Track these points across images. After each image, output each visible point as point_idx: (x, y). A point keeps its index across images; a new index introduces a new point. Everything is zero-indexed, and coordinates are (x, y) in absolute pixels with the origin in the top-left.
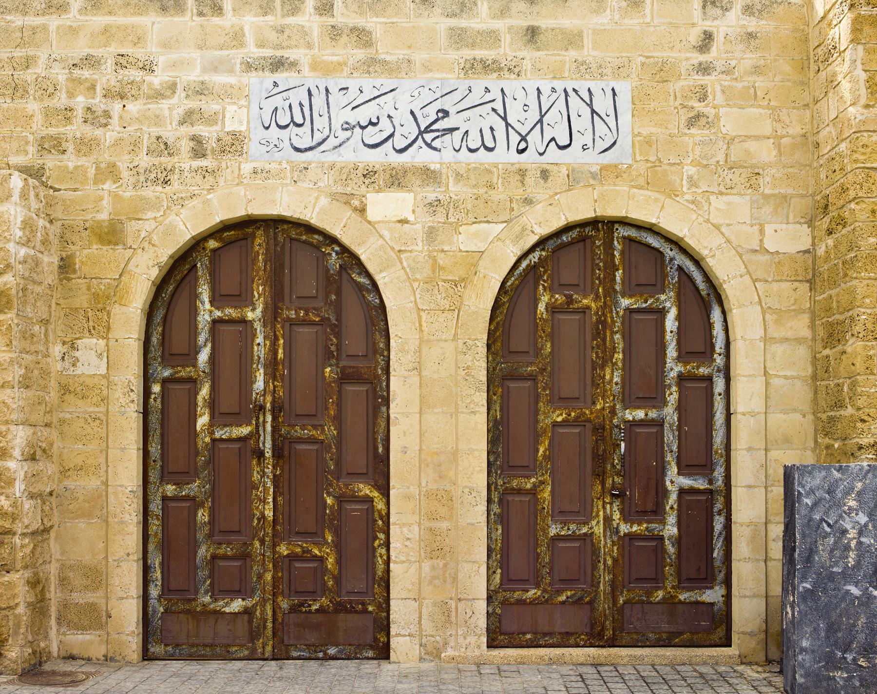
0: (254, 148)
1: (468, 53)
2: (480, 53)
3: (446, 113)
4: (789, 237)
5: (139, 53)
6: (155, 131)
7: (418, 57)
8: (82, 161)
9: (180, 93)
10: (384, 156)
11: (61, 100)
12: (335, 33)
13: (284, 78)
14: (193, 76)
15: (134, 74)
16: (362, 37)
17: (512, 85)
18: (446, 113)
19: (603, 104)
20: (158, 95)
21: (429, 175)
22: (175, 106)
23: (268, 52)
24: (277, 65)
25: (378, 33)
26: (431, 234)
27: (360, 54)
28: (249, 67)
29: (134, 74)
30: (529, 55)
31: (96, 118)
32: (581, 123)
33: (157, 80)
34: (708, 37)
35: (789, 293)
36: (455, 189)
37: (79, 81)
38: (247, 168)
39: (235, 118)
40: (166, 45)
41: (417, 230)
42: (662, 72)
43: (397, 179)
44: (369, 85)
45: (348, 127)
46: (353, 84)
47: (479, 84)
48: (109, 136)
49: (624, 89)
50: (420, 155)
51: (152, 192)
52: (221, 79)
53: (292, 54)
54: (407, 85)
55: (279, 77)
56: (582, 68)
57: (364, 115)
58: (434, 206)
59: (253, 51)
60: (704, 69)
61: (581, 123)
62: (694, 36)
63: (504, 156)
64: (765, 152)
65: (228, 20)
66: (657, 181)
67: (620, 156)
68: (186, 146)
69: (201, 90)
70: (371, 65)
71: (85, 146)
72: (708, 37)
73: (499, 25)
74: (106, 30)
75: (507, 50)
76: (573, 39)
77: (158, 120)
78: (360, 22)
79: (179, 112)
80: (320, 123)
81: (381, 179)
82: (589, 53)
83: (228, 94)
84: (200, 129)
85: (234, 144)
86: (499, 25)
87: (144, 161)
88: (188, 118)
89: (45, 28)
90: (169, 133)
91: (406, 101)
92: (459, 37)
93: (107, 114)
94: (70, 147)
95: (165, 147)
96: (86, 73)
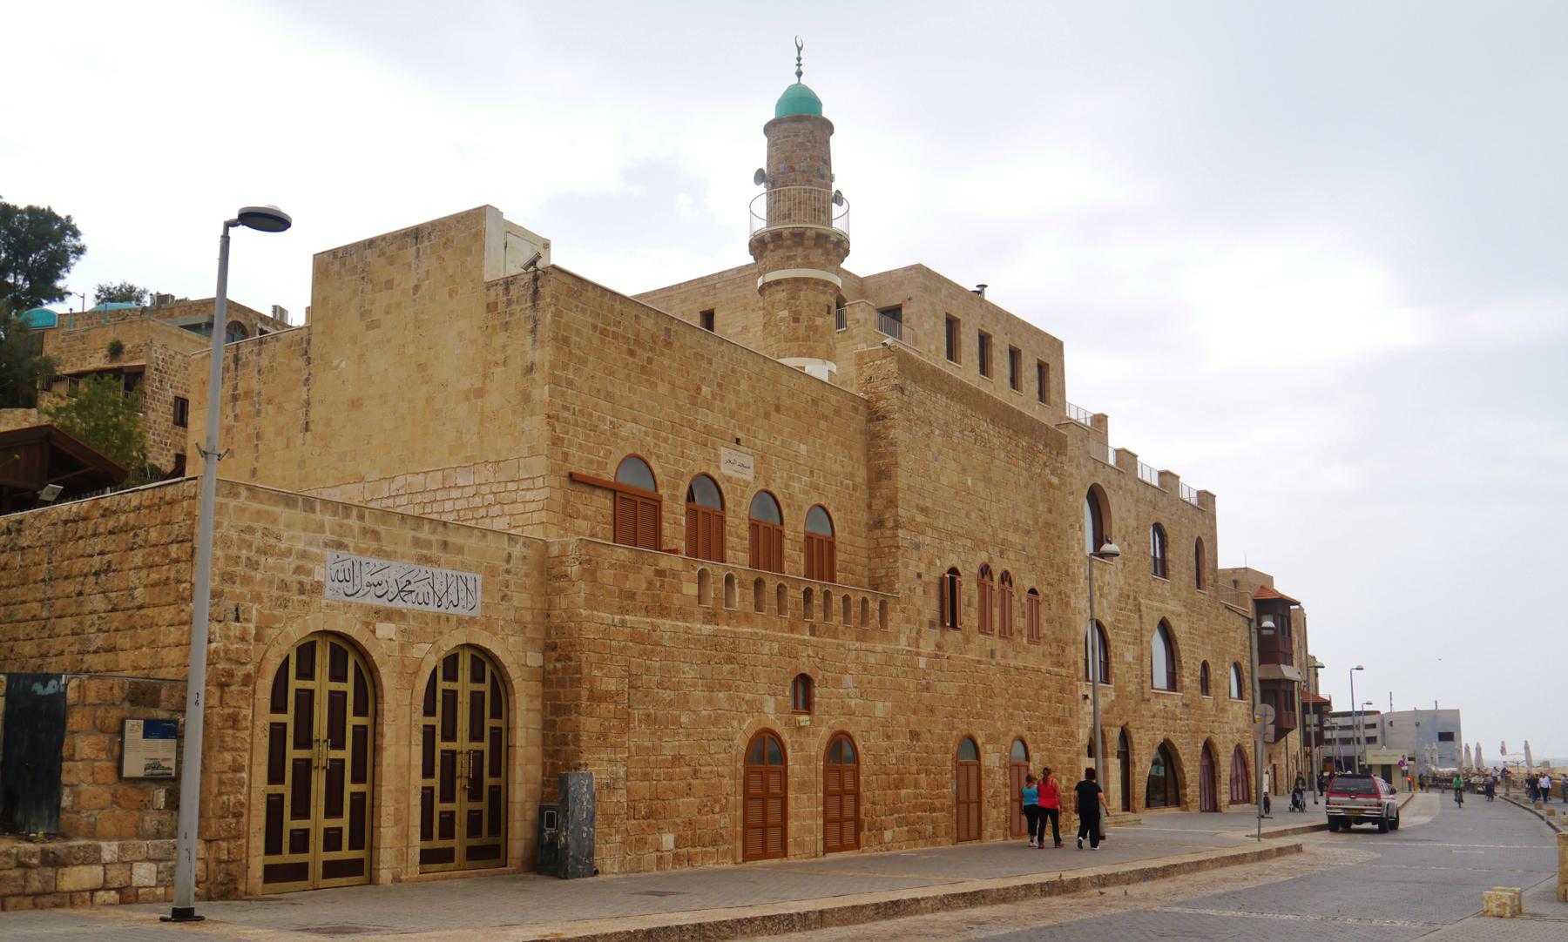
0: (327, 592)
1: (420, 551)
2: (425, 552)
3: (409, 582)
4: (535, 659)
5: (274, 528)
6: (281, 576)
7: (400, 550)
8: (244, 590)
9: (294, 555)
10: (382, 603)
11: (234, 551)
12: (365, 531)
13: (343, 554)
14: (300, 546)
15: (272, 541)
16: (376, 535)
17: (436, 570)
18: (409, 582)
19: (471, 586)
20: (283, 555)
21: (401, 615)
22: (291, 563)
23: (334, 538)
24: (340, 546)
25: (383, 534)
26: (402, 647)
27: (375, 545)
28: (326, 545)
29: (272, 541)
30: (444, 557)
31: (252, 564)
32: (462, 594)
33: (283, 546)
34: (510, 556)
35: (535, 687)
36: (413, 624)
37: (244, 541)
38: (324, 602)
39: (319, 574)
40: (289, 526)
41: (396, 644)
42: (492, 571)
43: (389, 615)
44: (379, 562)
45: (369, 585)
46: (372, 561)
47: (424, 568)
48: (258, 576)
49: (479, 578)
50: (398, 604)
51: (279, 612)
52: (314, 550)
53: (346, 541)
54: (394, 564)
55: (340, 552)
56: (464, 566)
57: (375, 579)
58: (403, 632)
59: (328, 536)
60: (508, 572)
61: (462, 594)
62: (505, 556)
63: (432, 608)
64: (528, 617)
65: (317, 516)
66: (488, 625)
67: (477, 613)
68: (295, 586)
69: (303, 555)
70: (380, 553)
71: (247, 581)
72: (510, 556)
73: (432, 538)
74: (259, 512)
75: (435, 551)
76: (460, 550)
77: (282, 569)
78: (376, 527)
79: (293, 566)
80: (357, 581)
81: (382, 615)
82: (467, 558)
83: (319, 559)
84: (303, 578)
85: (318, 588)
86: (432, 538)
87: (275, 593)
88: (298, 570)
89: (227, 505)
90: (289, 578)
91: (394, 572)
92: (417, 542)
93: (257, 563)
94: (238, 580)
95: (284, 586)
96: (248, 537)
